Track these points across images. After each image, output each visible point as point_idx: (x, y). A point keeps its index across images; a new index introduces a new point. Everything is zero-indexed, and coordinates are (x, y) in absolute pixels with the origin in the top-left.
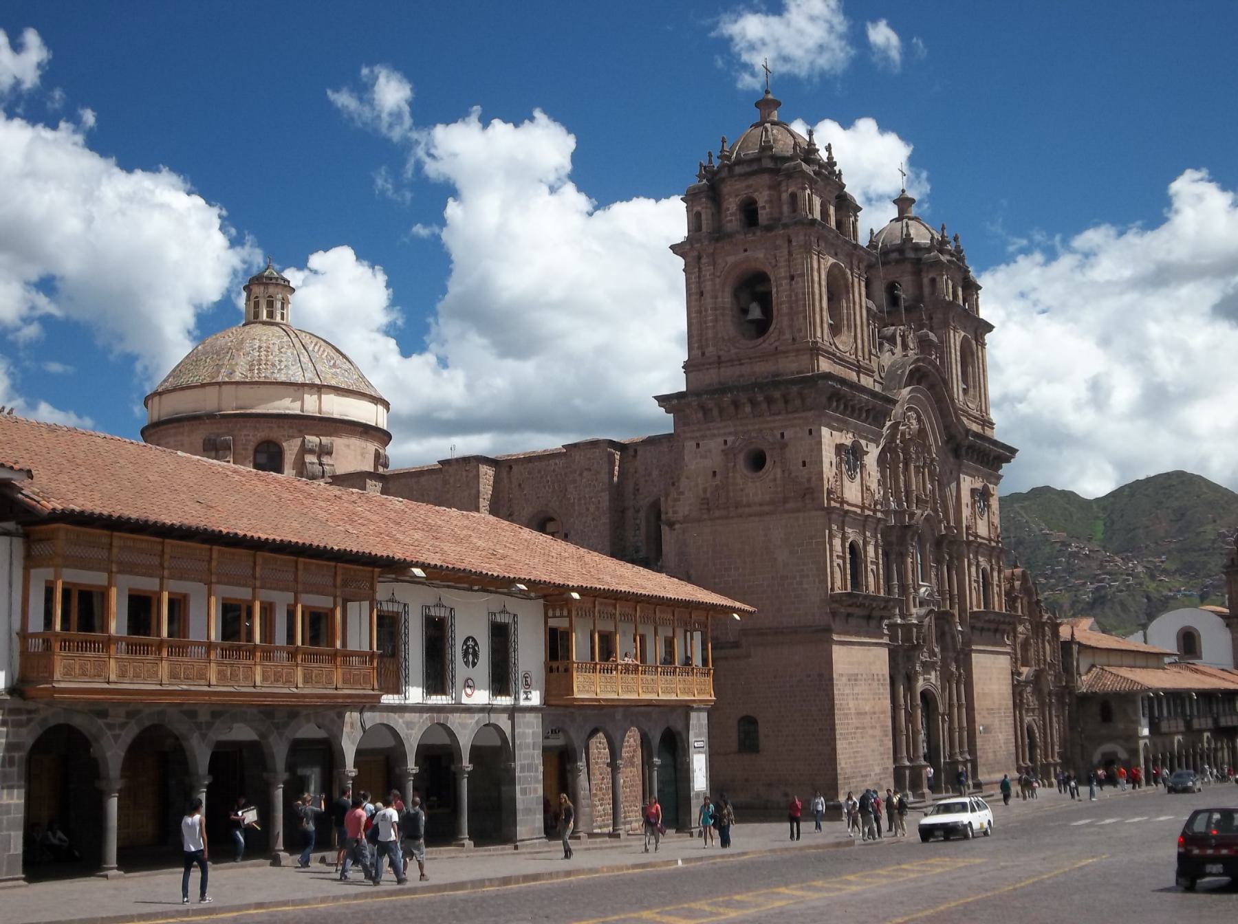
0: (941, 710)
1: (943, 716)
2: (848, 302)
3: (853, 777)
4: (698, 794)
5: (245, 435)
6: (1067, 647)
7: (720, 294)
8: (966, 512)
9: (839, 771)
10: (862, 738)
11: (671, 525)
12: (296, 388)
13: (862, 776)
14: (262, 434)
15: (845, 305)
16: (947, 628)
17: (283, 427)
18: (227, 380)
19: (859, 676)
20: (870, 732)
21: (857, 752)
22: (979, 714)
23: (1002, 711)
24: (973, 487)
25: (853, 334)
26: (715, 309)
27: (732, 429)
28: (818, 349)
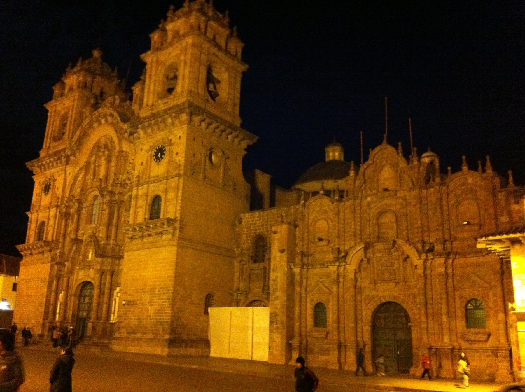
23: (157, 290)
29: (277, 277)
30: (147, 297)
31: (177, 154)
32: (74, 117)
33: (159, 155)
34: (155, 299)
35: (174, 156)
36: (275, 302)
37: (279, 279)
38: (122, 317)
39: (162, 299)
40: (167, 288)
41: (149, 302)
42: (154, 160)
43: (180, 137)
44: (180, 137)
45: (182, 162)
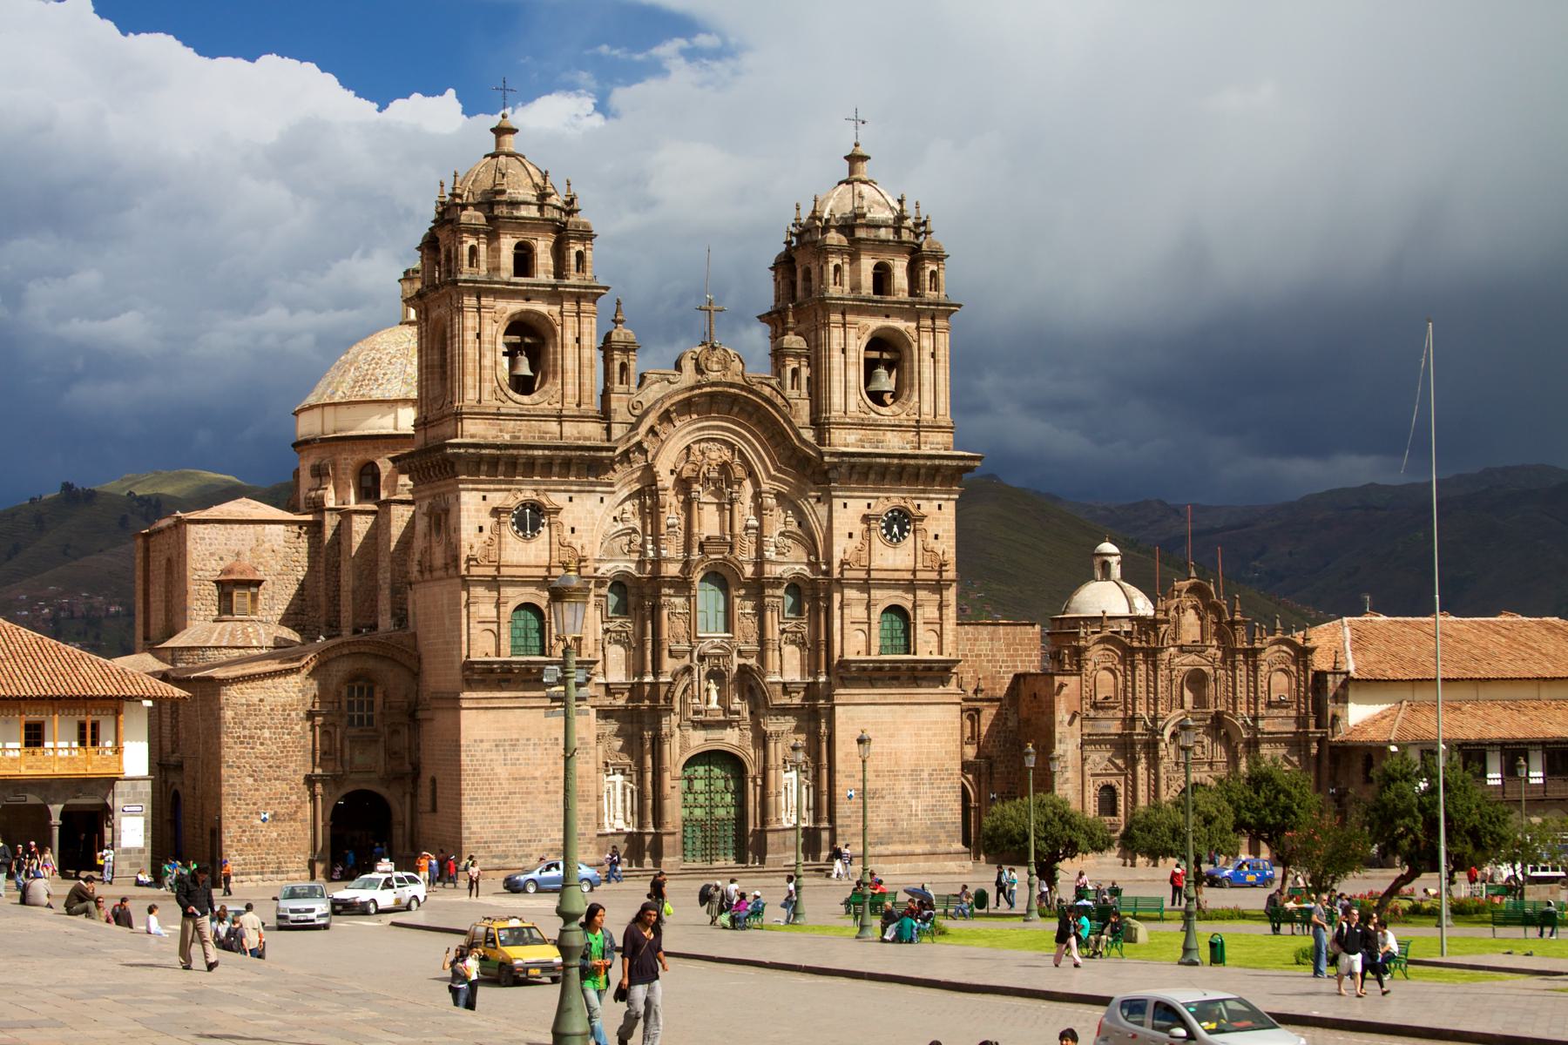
0: (752, 771)
1: (754, 778)
2: (555, 345)
3: (500, 842)
4: (127, 851)
5: (345, 459)
6: (1320, 676)
7: (429, 351)
8: (841, 548)
9: (465, 833)
10: (523, 803)
11: (410, 584)
12: (390, 405)
13: (519, 841)
14: (361, 456)
15: (551, 350)
16: (753, 683)
17: (378, 448)
18: (328, 401)
19: (521, 742)
20: (542, 796)
21: (510, 817)
22: (846, 776)
23: (925, 775)
24: (867, 511)
25: (560, 382)
26: (427, 367)
27: (428, 493)
28: (462, 414)
29: (1066, 751)
30: (905, 786)
31: (936, 537)
32: (586, 353)
33: (896, 529)
34: (925, 788)
35: (931, 540)
36: (1066, 786)
37: (1069, 754)
38: (849, 817)
39: (939, 788)
40: (947, 770)
41: (910, 793)
42: (885, 535)
43: (940, 507)
44: (940, 507)
45: (951, 556)
